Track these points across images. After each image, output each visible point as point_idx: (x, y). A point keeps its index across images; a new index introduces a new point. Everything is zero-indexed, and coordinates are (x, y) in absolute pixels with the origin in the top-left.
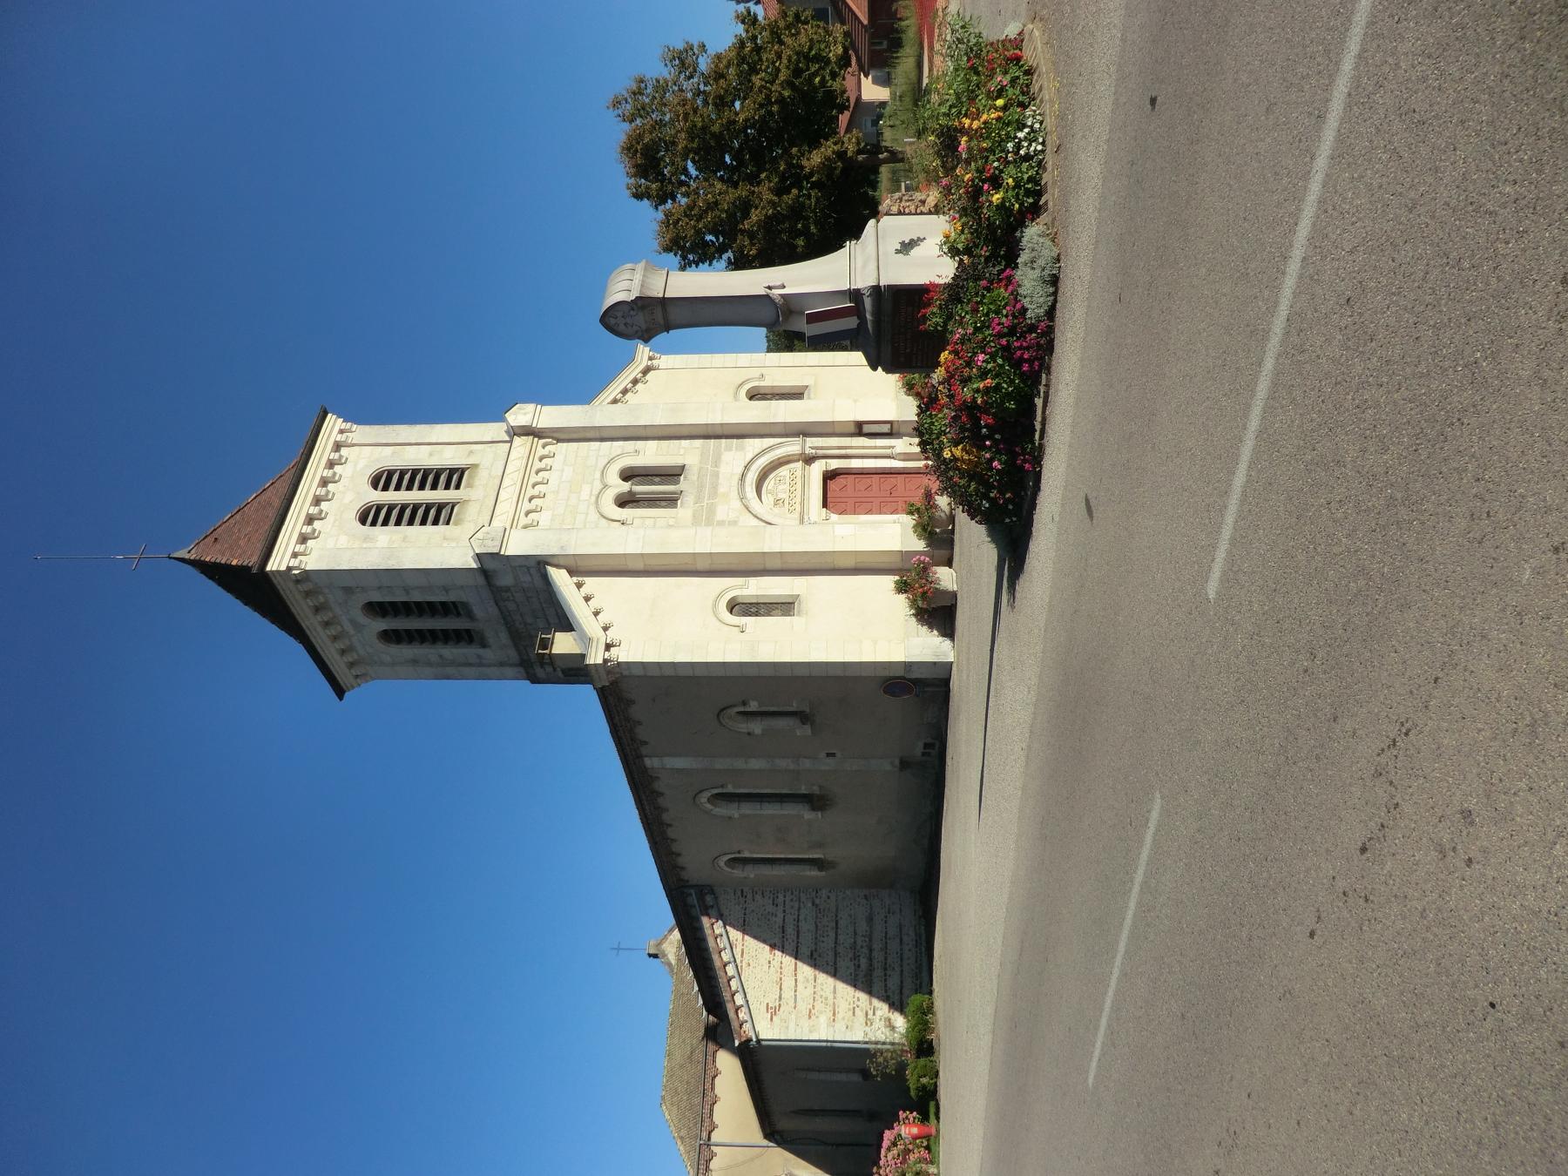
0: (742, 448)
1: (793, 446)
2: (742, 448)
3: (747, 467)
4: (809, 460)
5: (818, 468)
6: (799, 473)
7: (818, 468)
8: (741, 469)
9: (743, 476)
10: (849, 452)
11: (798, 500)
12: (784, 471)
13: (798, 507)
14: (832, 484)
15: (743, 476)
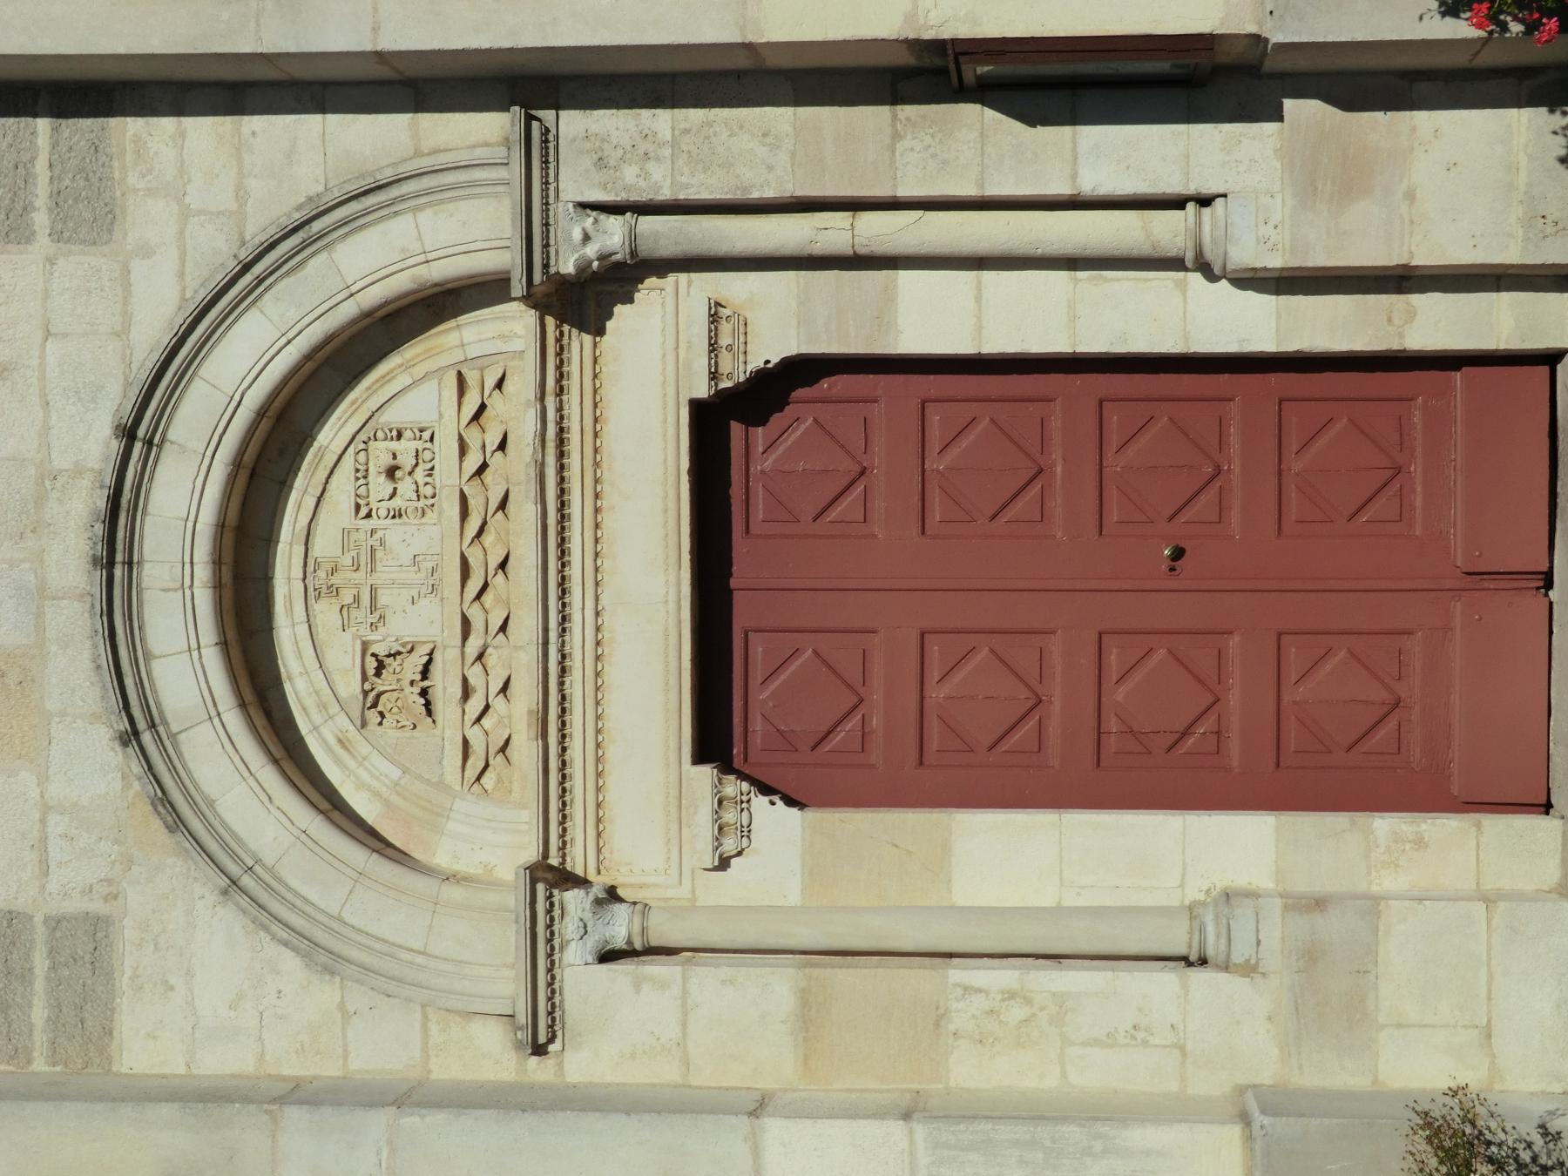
0: (90, 216)
1: (453, 201)
2: (90, 216)
3: (138, 434)
4: (582, 301)
5: (653, 360)
6: (516, 412)
7: (653, 360)
8: (96, 445)
9: (119, 512)
10: (876, 230)
11: (518, 657)
12: (410, 390)
13: (526, 750)
14: (761, 452)
15: (119, 512)
